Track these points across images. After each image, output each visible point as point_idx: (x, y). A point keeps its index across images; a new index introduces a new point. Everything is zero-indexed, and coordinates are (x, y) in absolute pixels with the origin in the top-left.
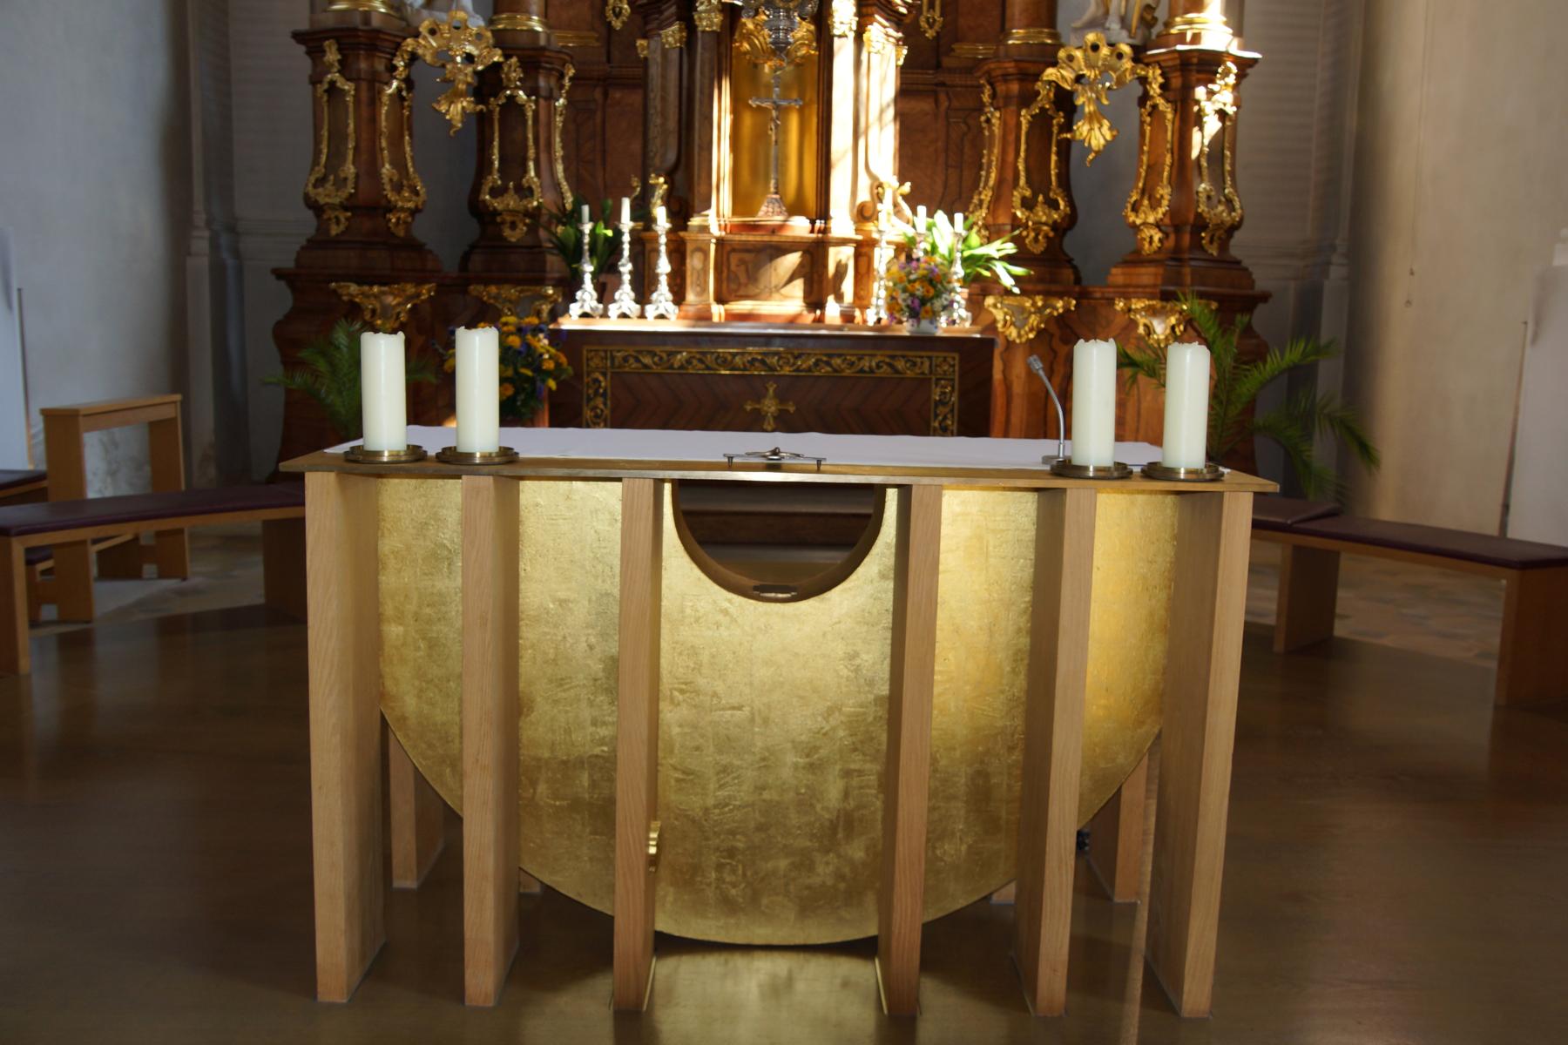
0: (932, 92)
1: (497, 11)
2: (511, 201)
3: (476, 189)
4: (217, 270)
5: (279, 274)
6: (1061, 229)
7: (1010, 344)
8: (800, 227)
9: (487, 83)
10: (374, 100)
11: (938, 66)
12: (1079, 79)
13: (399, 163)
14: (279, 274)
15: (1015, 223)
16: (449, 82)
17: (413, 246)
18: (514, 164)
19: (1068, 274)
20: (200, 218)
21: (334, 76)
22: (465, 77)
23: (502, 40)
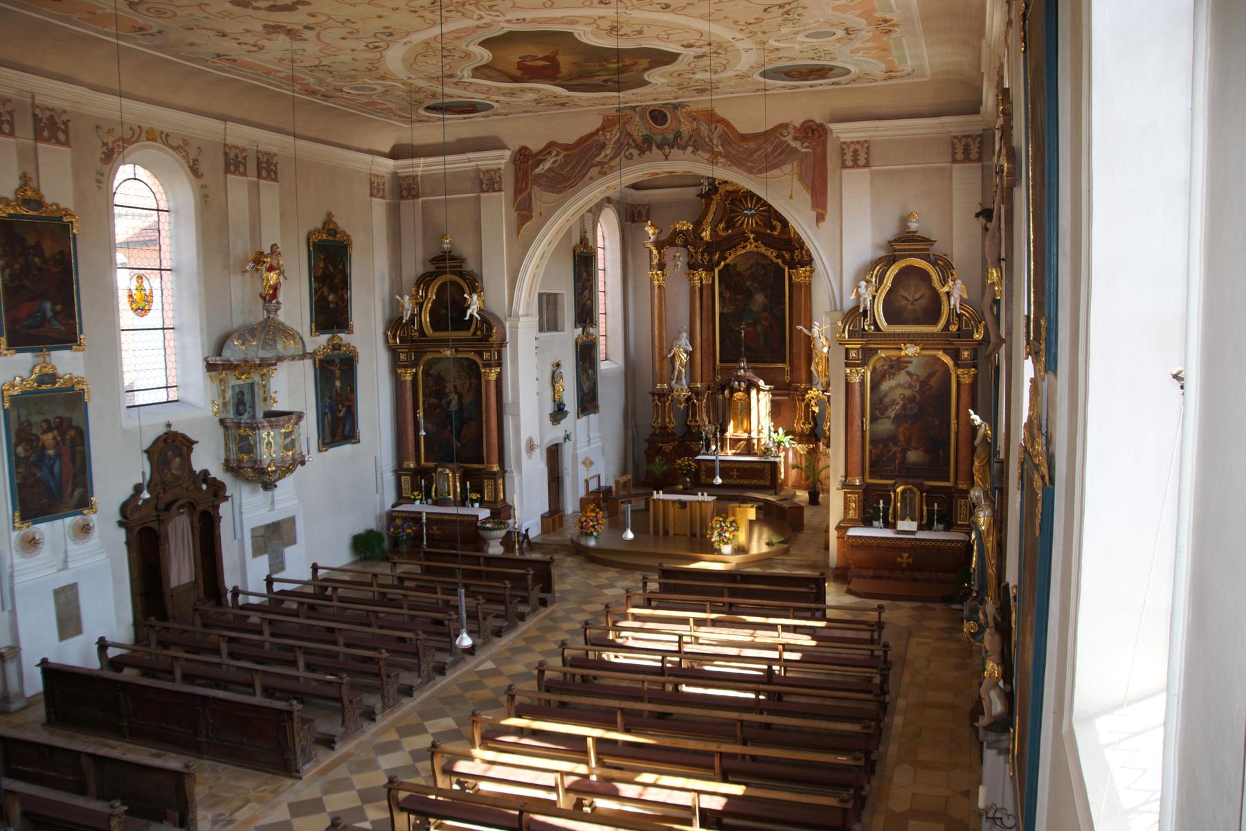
0: (788, 395)
1: (691, 382)
2: (693, 423)
3: (686, 421)
4: (633, 438)
5: (646, 440)
6: (813, 429)
7: (801, 455)
8: (745, 436)
9: (688, 399)
10: (665, 407)
11: (789, 390)
12: (813, 398)
13: (670, 418)
14: (646, 440)
15: (802, 429)
16: (680, 400)
17: (673, 434)
18: (694, 415)
19: (814, 439)
20: (630, 426)
21: (657, 402)
22: (683, 399)
23: (691, 389)
